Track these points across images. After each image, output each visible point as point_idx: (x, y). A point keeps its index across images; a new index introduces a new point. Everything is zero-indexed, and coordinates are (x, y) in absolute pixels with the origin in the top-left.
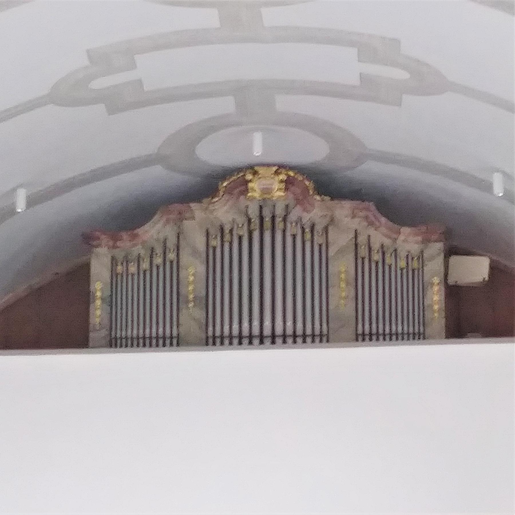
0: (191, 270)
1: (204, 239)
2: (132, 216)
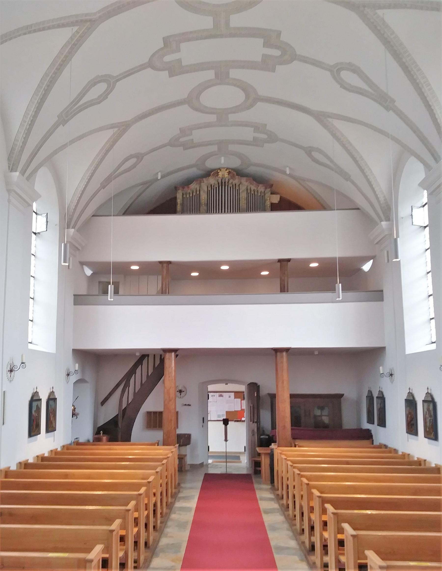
2: (187, 182)
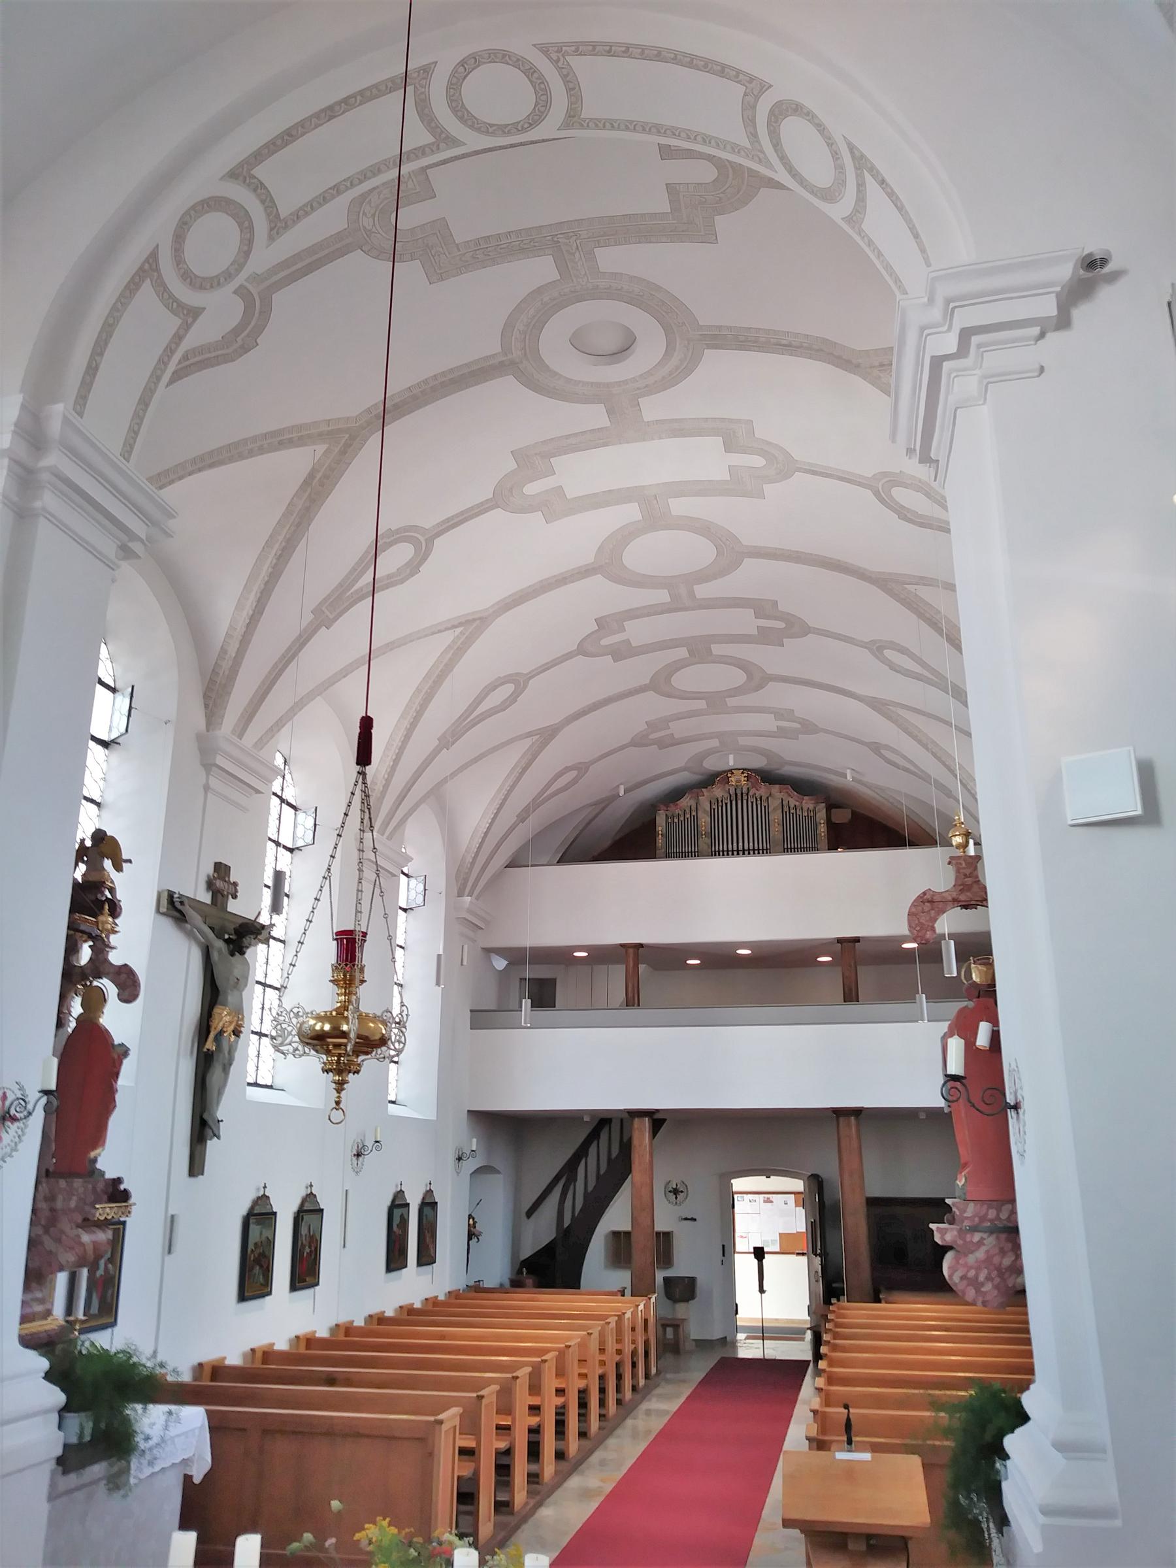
2: (675, 795)
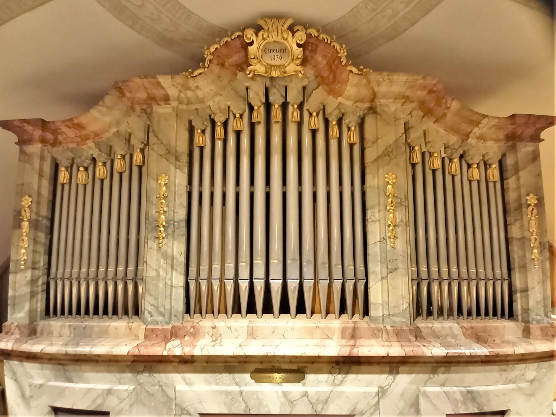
0: (163, 180)
1: (185, 135)
